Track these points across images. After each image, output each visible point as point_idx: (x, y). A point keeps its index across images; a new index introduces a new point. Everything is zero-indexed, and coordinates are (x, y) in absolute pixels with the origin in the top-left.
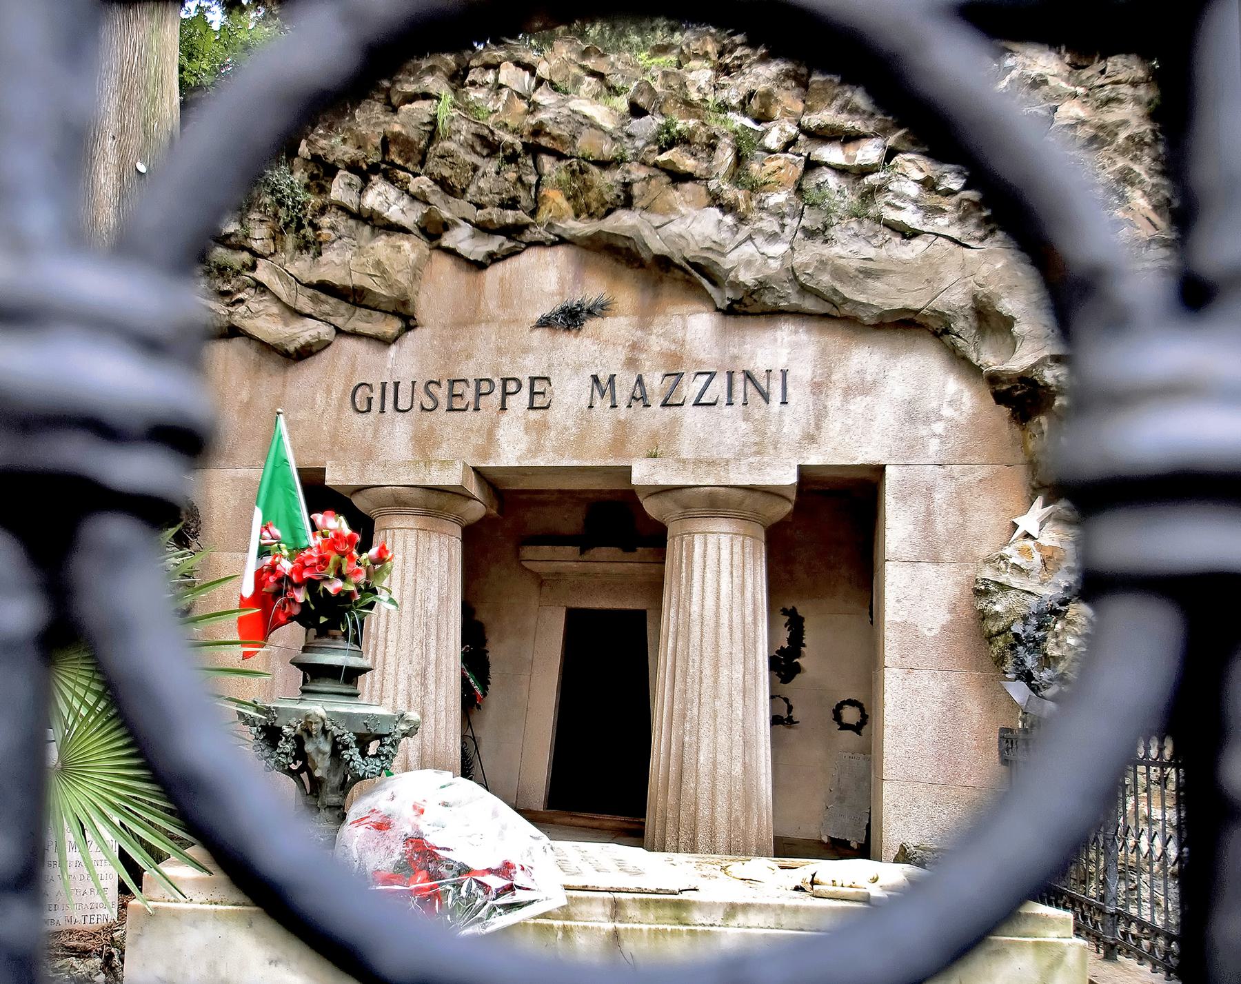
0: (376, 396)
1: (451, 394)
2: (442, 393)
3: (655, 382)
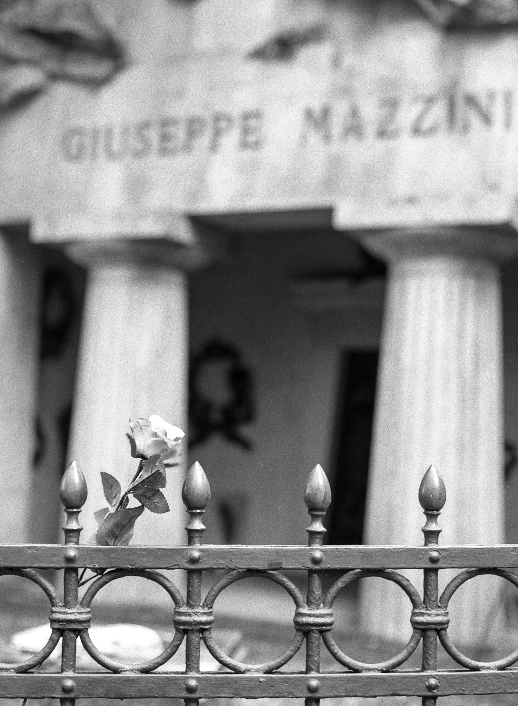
0: (88, 141)
1: (164, 135)
2: (153, 135)
3: (370, 111)
